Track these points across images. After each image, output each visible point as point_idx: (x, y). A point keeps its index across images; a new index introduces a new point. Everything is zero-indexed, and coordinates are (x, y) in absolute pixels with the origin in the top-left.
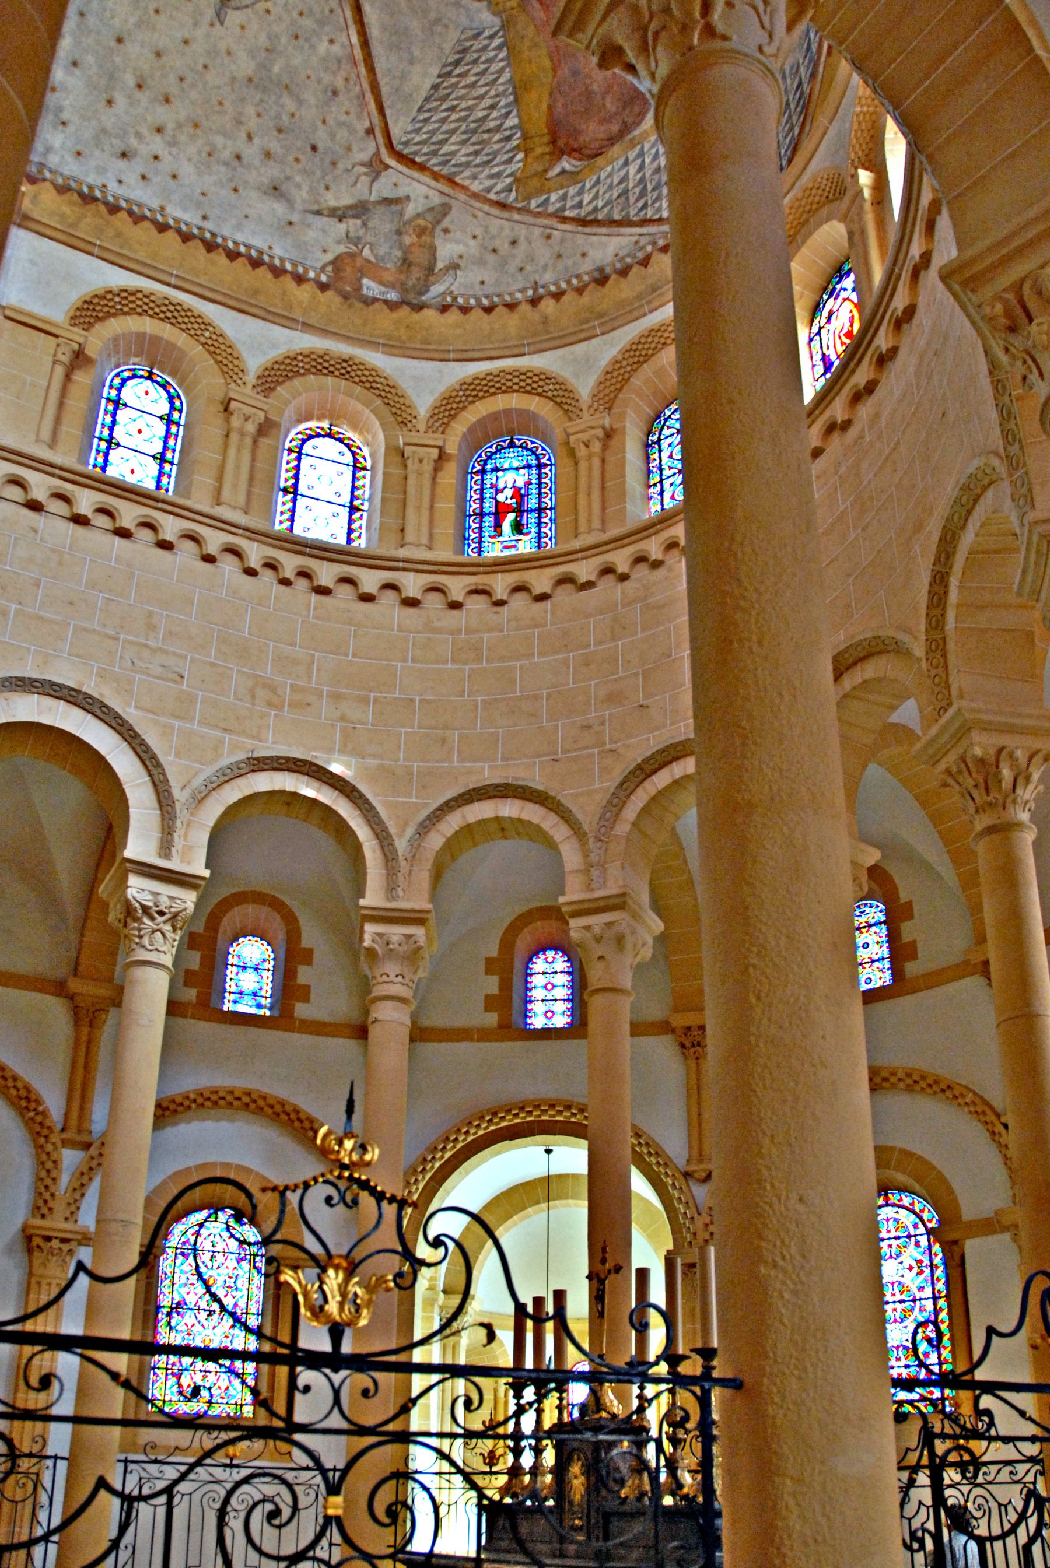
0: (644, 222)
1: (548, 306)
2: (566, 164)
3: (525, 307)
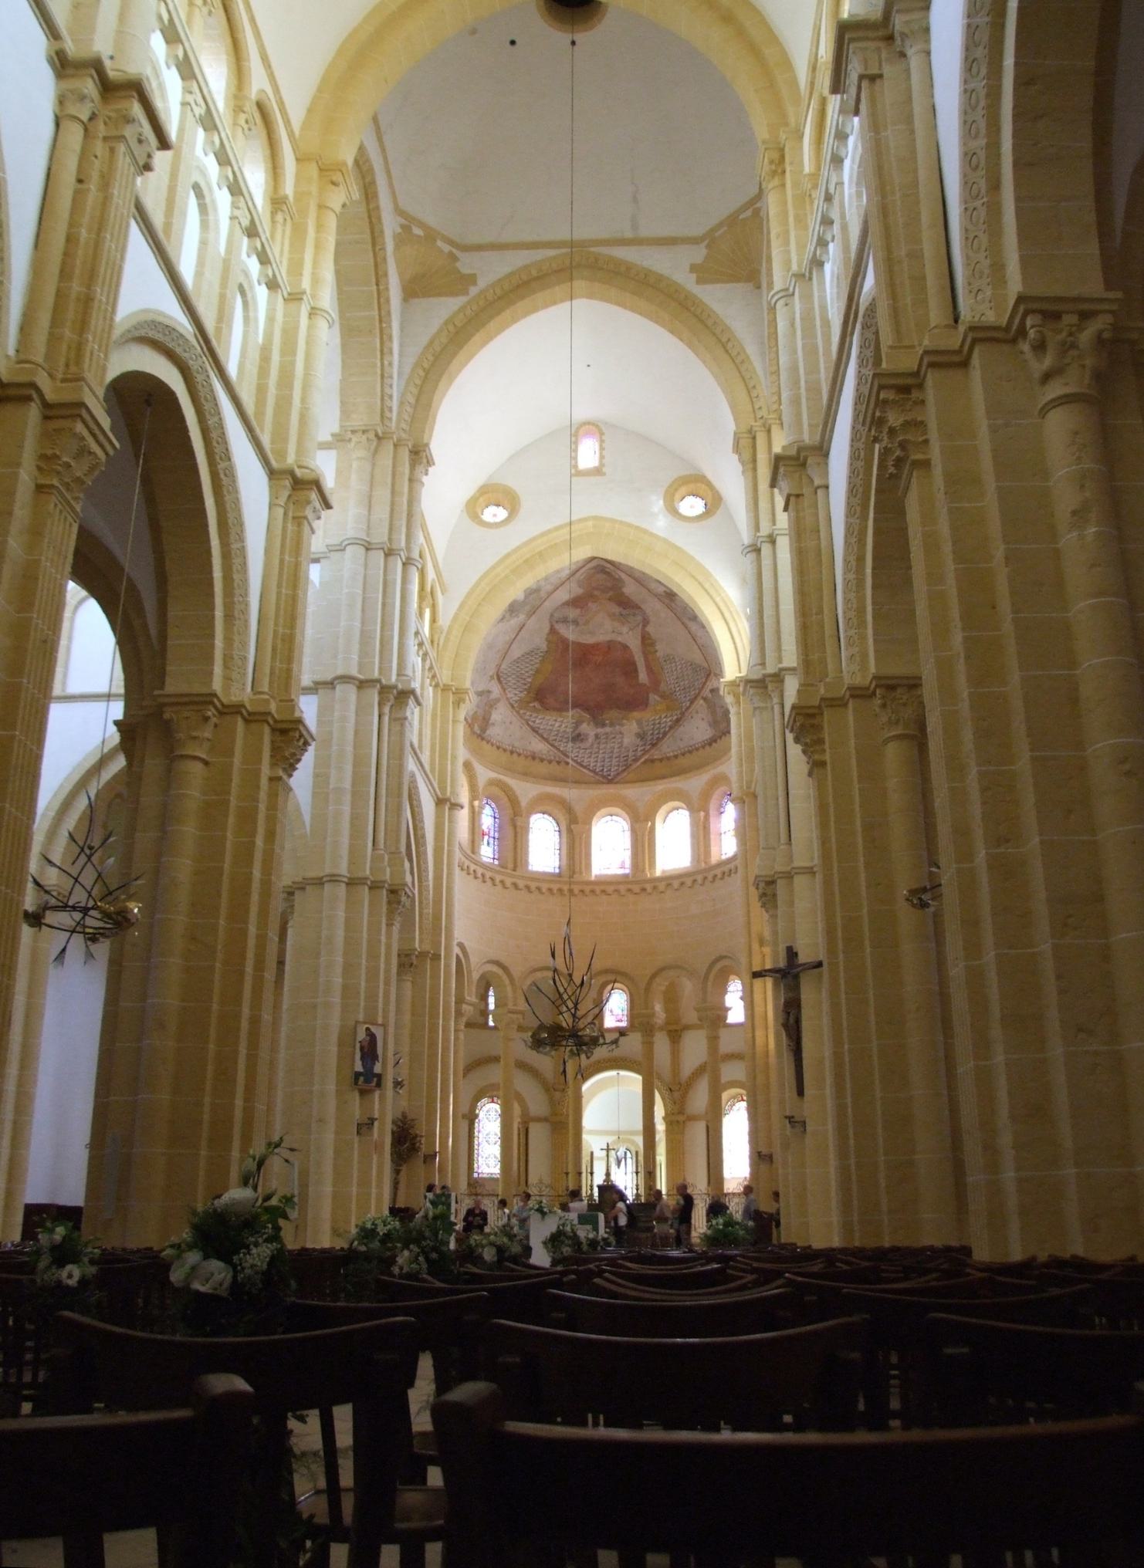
0: (552, 745)
1: (515, 755)
2: (536, 704)
3: (509, 753)
